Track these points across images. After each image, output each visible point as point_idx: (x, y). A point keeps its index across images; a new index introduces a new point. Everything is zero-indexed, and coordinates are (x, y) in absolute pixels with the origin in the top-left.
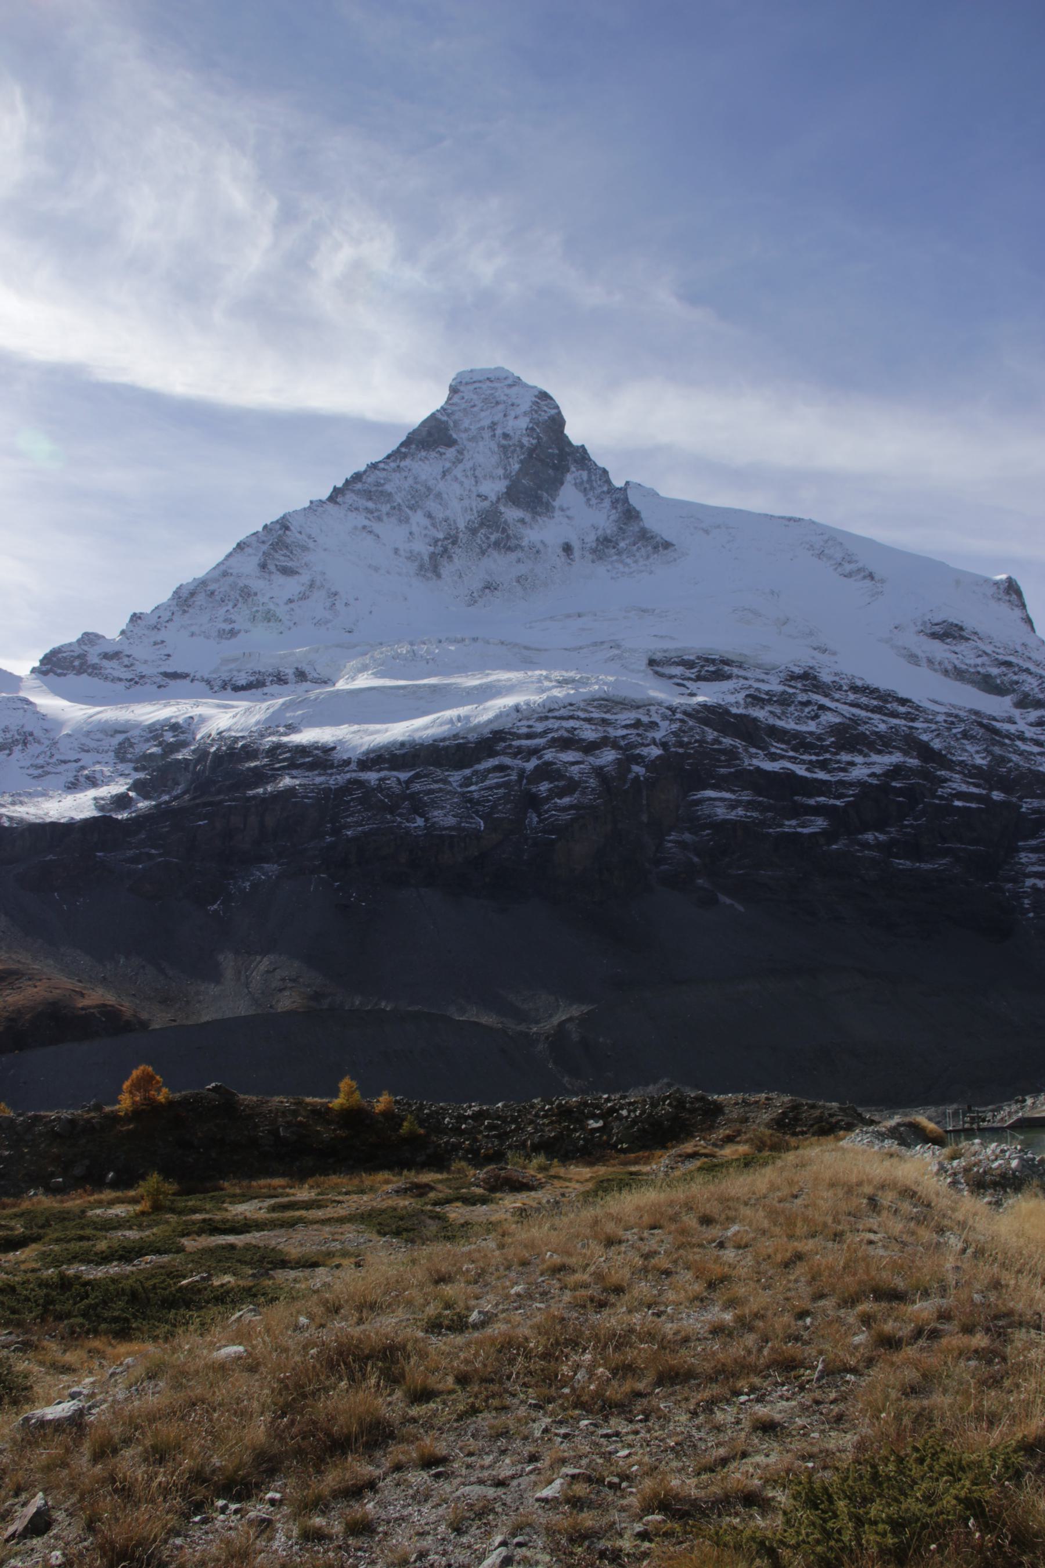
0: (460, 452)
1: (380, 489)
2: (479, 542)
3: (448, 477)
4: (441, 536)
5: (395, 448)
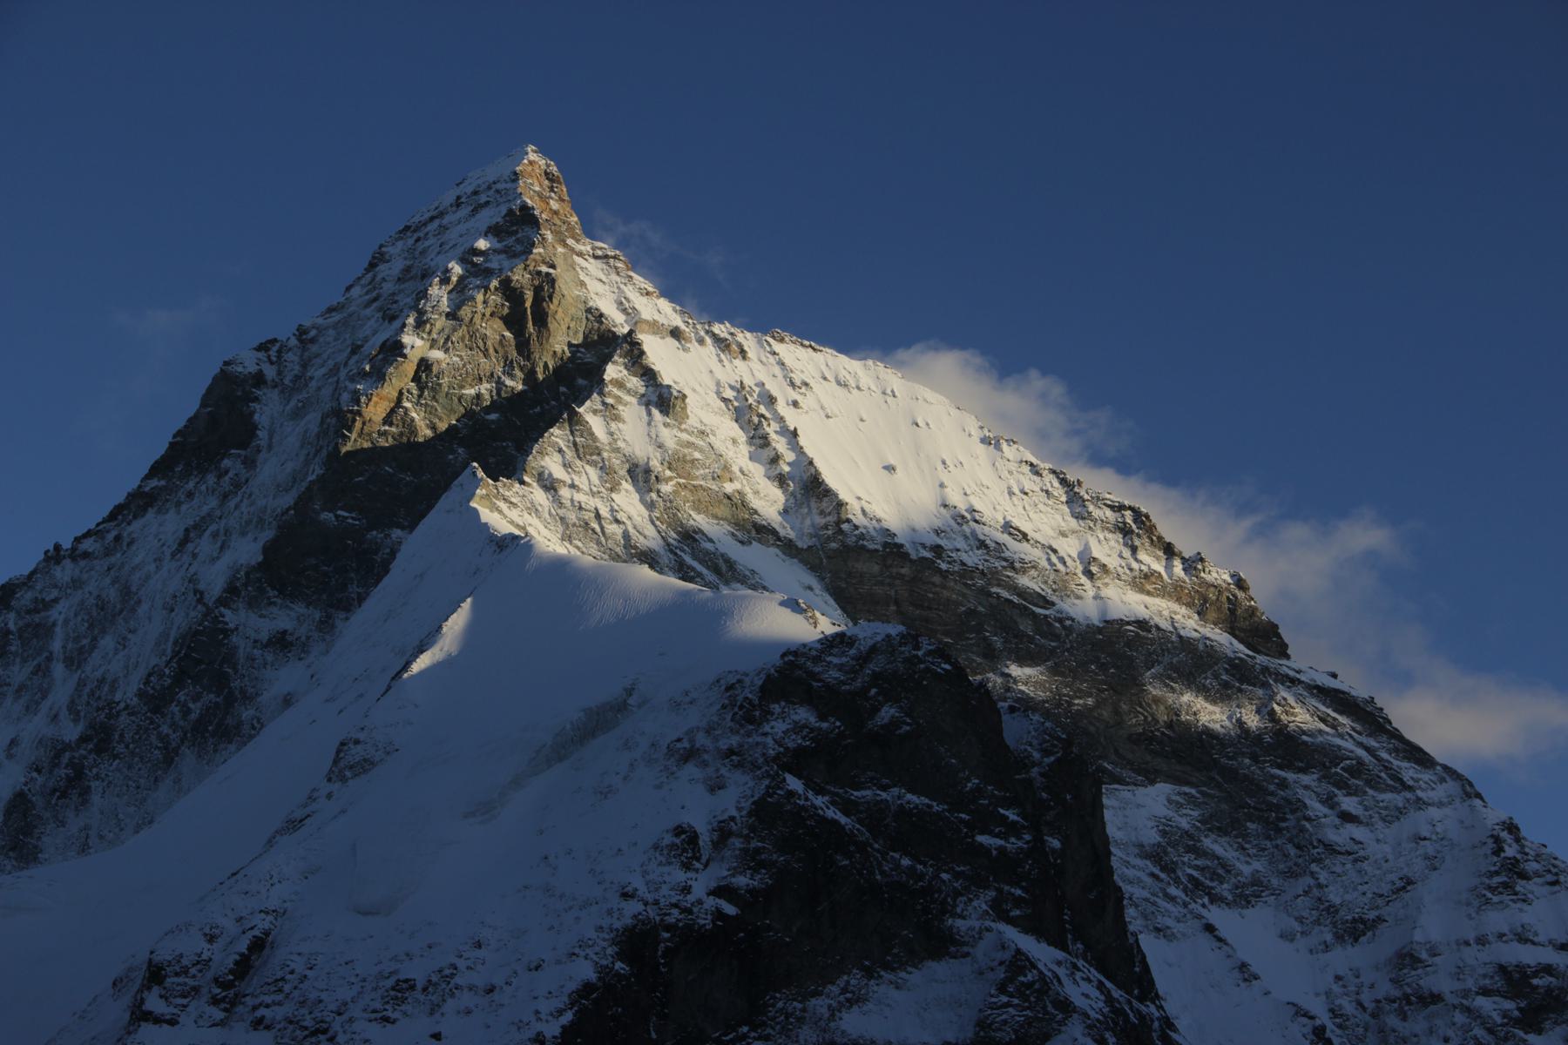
0: (250, 463)
1: (37, 618)
2: (165, 729)
3: (190, 546)
4: (71, 732)
5: (132, 484)
